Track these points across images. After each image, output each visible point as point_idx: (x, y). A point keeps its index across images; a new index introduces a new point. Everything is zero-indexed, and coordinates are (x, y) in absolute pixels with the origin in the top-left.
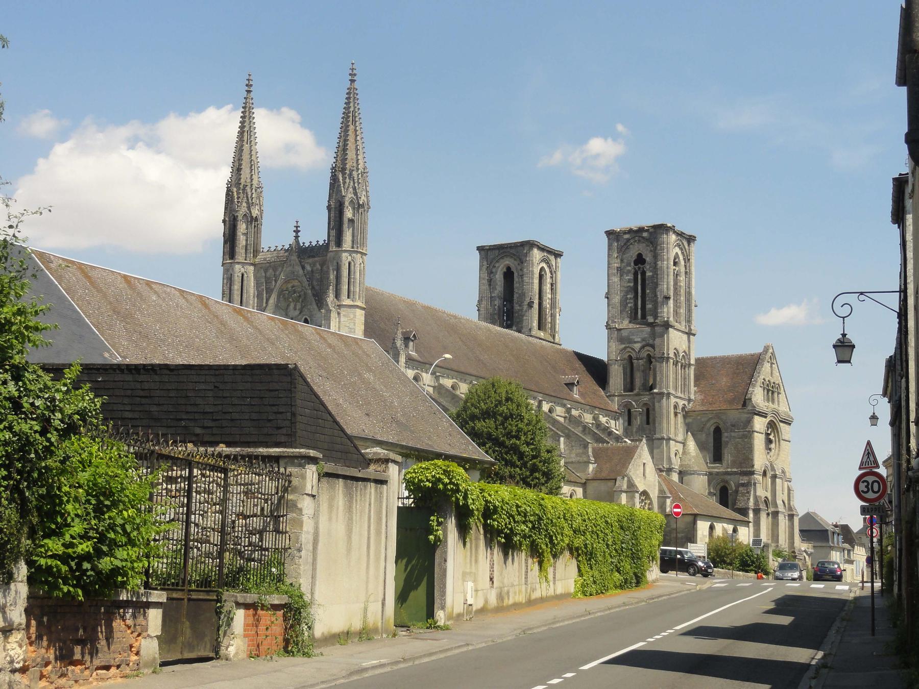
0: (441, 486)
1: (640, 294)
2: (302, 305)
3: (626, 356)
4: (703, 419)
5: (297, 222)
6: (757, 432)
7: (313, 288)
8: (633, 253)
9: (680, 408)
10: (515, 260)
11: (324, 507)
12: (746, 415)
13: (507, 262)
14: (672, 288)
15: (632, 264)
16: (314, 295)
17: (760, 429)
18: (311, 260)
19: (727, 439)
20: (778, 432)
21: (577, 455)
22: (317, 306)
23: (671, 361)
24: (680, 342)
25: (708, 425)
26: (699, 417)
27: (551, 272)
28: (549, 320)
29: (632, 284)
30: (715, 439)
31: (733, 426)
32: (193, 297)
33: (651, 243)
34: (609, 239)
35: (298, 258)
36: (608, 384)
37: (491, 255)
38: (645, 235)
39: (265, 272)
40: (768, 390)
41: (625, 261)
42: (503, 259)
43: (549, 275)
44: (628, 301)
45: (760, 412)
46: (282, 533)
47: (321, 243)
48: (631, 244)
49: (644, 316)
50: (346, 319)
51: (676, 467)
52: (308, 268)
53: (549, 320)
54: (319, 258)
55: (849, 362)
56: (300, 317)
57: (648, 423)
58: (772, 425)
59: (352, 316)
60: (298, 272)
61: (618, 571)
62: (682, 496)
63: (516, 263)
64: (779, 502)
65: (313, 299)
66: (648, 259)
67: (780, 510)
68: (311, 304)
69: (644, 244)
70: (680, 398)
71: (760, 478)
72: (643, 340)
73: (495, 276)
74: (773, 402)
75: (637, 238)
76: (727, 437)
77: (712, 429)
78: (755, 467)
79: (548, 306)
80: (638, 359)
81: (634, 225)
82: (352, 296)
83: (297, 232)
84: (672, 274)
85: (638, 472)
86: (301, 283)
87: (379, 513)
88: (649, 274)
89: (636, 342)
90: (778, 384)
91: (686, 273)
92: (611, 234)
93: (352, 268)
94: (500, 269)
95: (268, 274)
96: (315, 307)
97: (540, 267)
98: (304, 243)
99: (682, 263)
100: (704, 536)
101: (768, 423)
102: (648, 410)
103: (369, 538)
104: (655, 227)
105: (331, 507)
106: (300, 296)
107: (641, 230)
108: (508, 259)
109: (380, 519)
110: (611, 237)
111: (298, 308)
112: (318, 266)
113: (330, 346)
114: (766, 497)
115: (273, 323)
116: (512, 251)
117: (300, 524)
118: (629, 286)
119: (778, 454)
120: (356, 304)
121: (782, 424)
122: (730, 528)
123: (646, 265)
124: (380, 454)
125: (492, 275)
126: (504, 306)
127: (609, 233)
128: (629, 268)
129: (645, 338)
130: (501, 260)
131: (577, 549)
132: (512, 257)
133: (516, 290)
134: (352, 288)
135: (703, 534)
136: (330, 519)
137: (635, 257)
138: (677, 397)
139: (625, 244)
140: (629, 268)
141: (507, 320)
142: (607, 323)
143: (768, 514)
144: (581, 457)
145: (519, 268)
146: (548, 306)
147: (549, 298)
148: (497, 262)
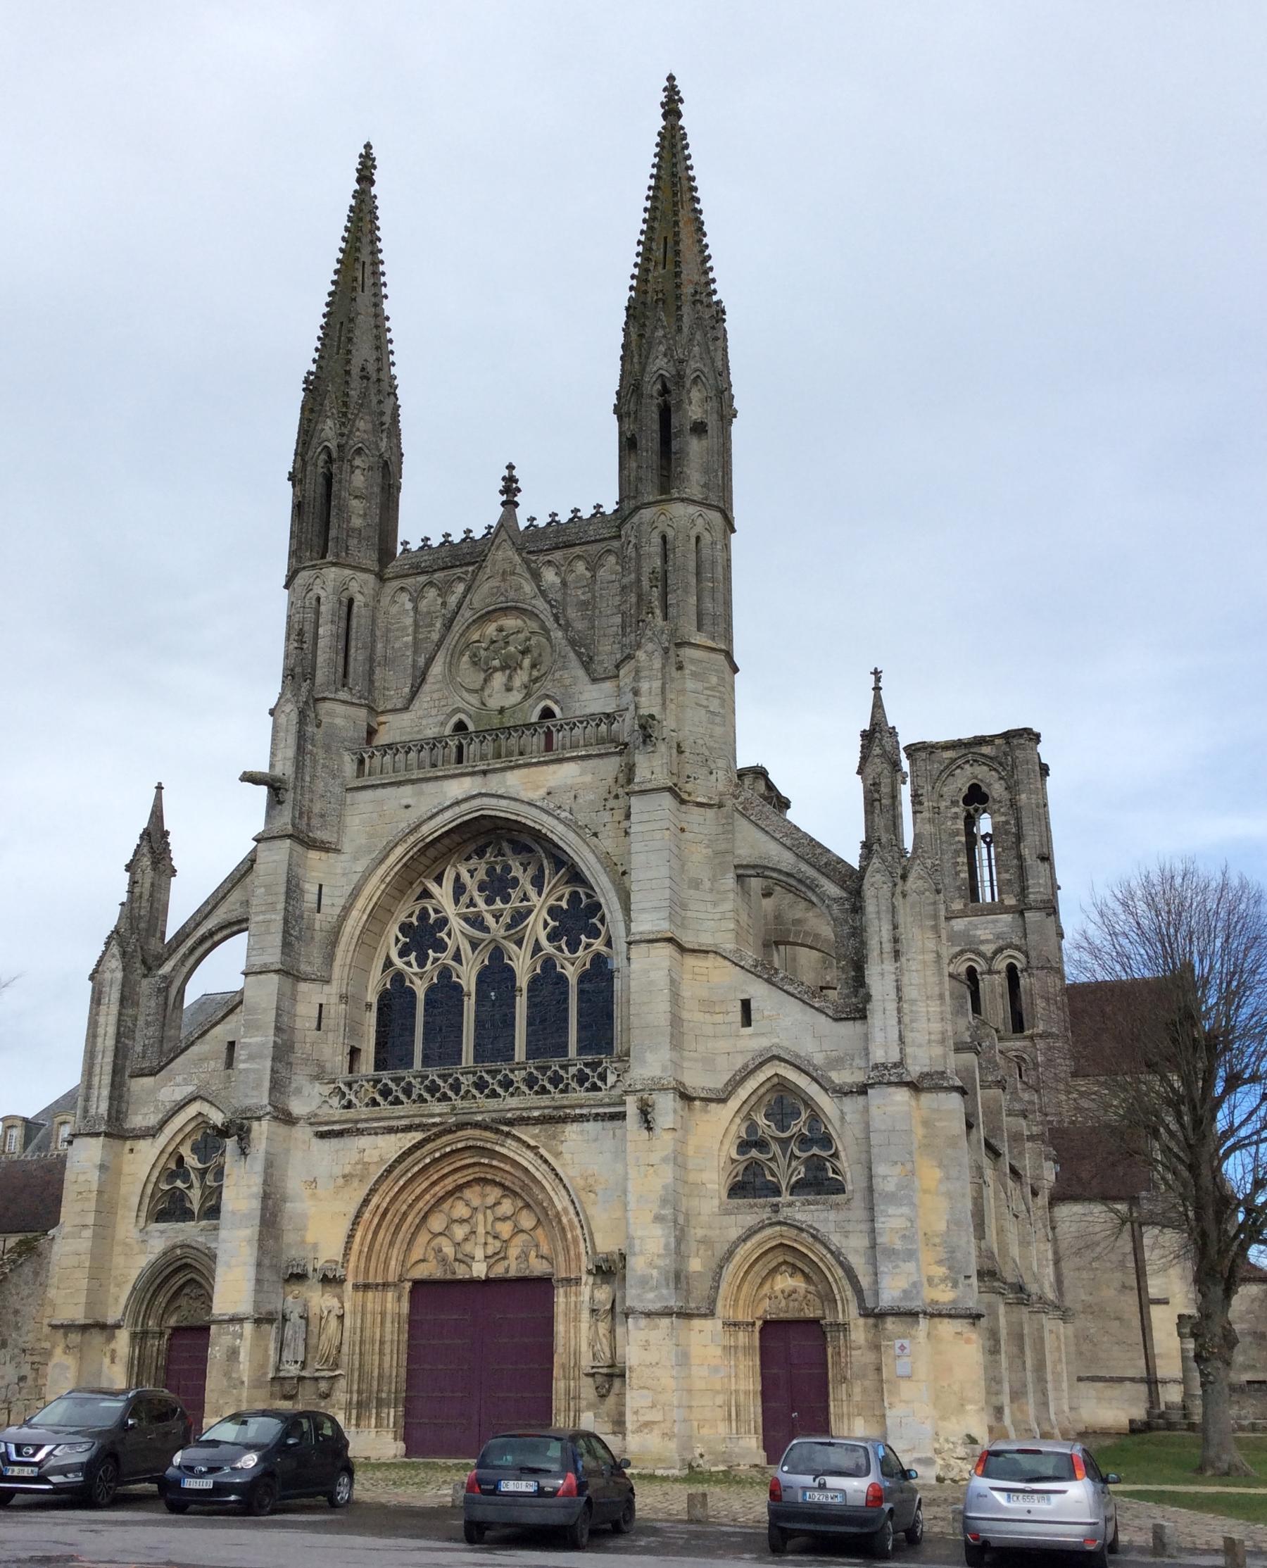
3: (963, 969)
8: (961, 782)
16: (572, 643)
18: (557, 556)
29: (963, 839)
33: (1001, 764)
38: (986, 750)
39: (414, 600)
48: (959, 767)
50: (699, 686)
52: (550, 576)
56: (527, 704)
59: (714, 680)
68: (564, 668)
72: (998, 937)
80: (990, 972)
81: (966, 733)
82: (708, 626)
89: (982, 942)
95: (423, 605)
96: (581, 673)
104: (1008, 736)
107: (980, 741)
123: (990, 803)
128: (955, 810)
137: (965, 790)
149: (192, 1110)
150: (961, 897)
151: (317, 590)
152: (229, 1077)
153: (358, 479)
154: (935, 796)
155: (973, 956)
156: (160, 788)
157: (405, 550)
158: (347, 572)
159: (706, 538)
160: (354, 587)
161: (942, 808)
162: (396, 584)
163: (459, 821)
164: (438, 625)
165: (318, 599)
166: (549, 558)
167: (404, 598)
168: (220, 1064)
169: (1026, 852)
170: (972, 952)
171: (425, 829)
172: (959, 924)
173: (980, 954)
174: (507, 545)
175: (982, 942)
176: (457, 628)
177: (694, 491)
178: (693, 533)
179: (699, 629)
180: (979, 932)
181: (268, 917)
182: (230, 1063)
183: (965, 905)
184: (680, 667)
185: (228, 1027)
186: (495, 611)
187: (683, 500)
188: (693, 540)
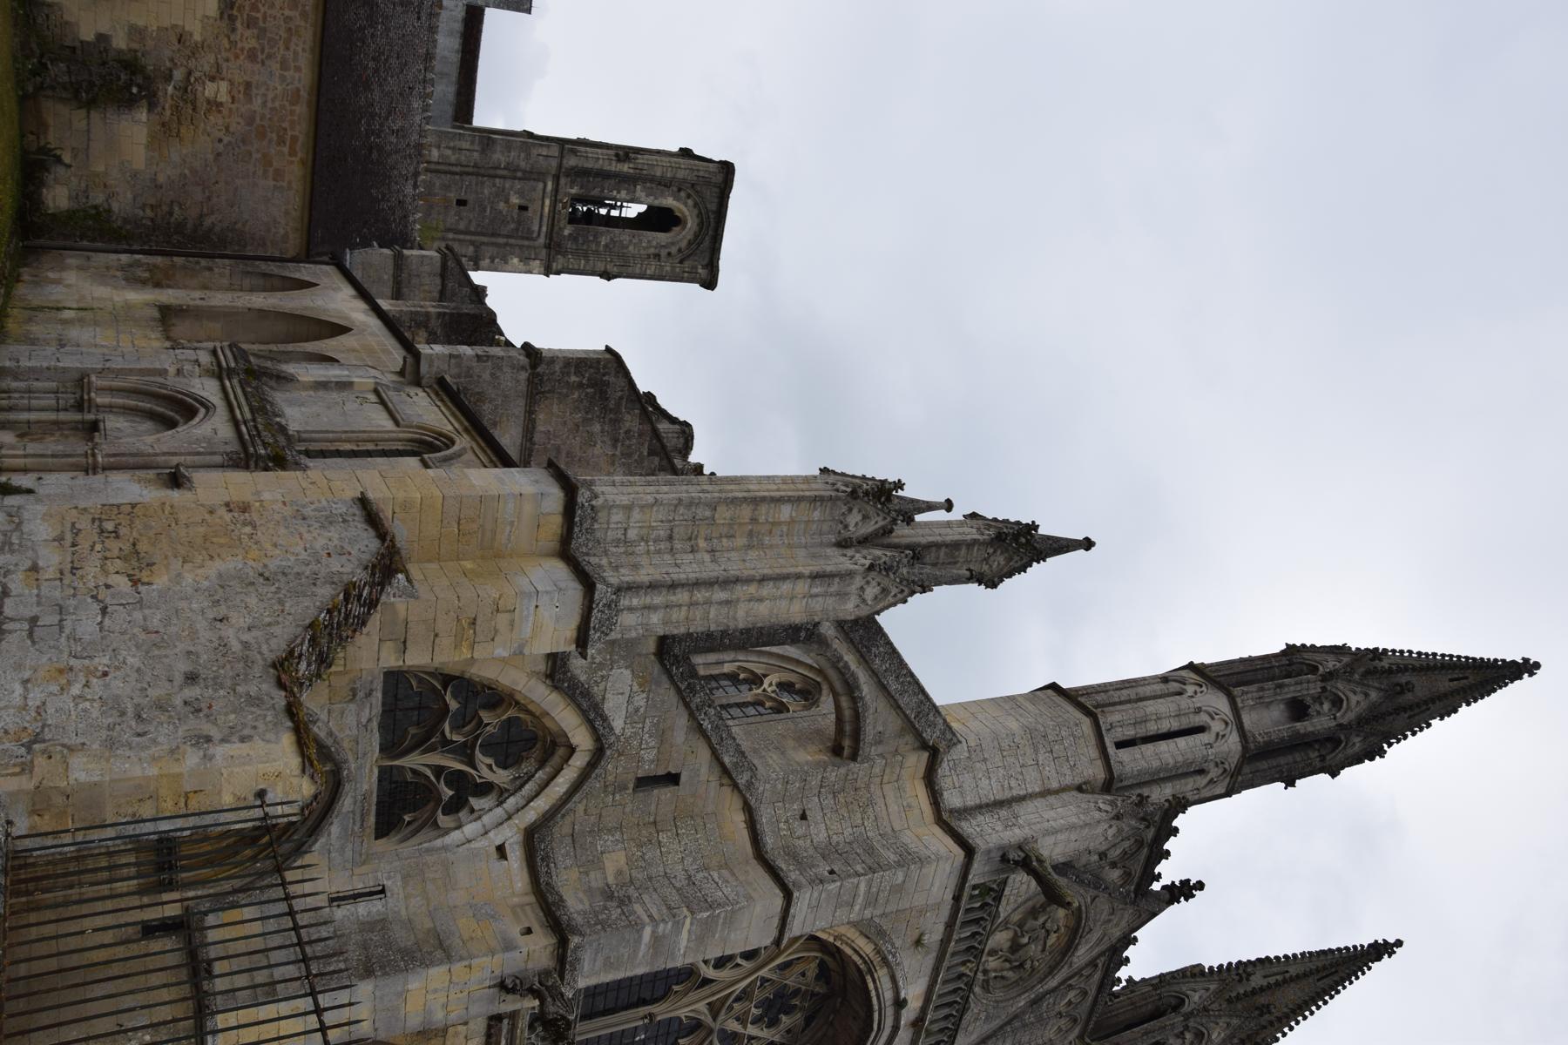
10: (690, 243)
13: (689, 225)
37: (710, 195)
42: (698, 216)
63: (684, 244)
108: (695, 228)
116: (707, 243)
130: (696, 212)
145: (674, 250)
148: (696, 205)
149: (581, 739)
152: (623, 788)
156: (1088, 544)
163: (876, 1007)
168: (647, 769)
171: (882, 974)
181: (860, 900)
182: (646, 782)
185: (704, 770)
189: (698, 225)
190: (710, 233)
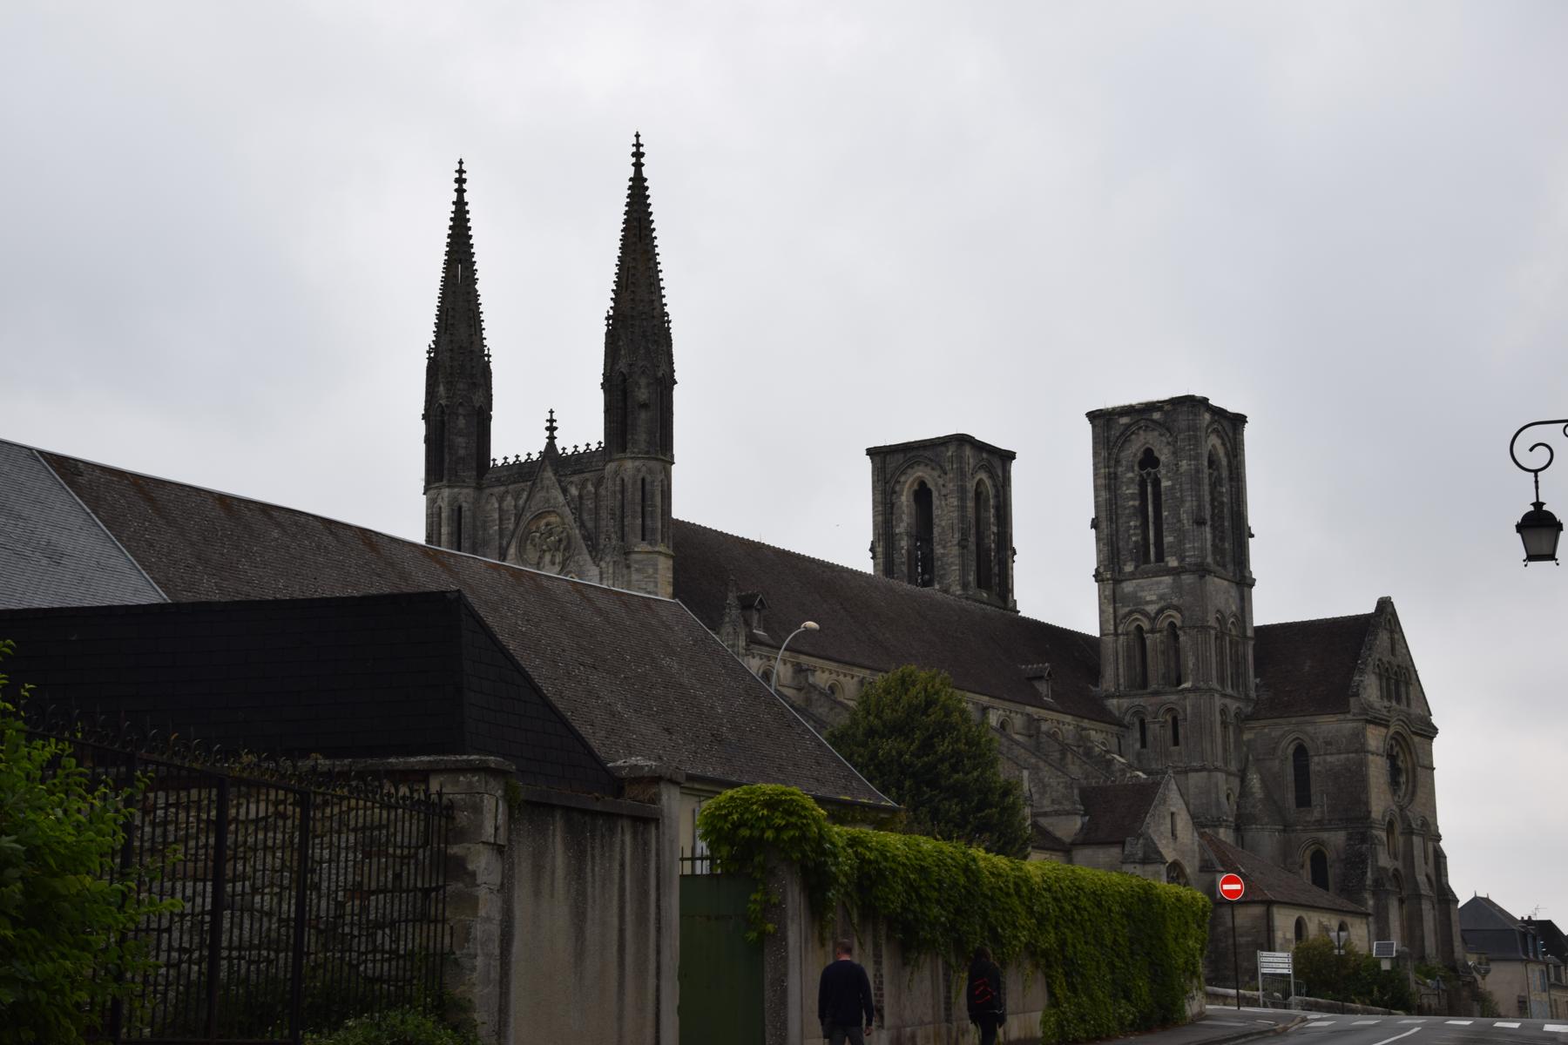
0: (769, 834)
1: (1151, 519)
2: (564, 555)
4: (1273, 734)
5: (551, 412)
6: (1373, 754)
7: (582, 525)
8: (1134, 449)
9: (1233, 714)
10: (933, 469)
11: (524, 869)
12: (1350, 725)
13: (920, 474)
14: (1208, 506)
15: (1136, 468)
17: (1378, 748)
18: (575, 478)
19: (1318, 768)
20: (1411, 753)
21: (1053, 802)
22: (591, 556)
23: (1213, 632)
24: (1227, 600)
25: (1284, 743)
26: (1266, 730)
27: (995, 486)
28: (996, 569)
29: (1137, 503)
30: (1296, 768)
31: (1328, 743)
32: (348, 533)
33: (1168, 429)
34: (1094, 427)
35: (555, 474)
36: (1103, 676)
38: (1156, 416)
40: (1388, 679)
41: (1124, 463)
42: (912, 468)
43: (991, 492)
44: (1132, 532)
45: (1376, 718)
46: (436, 921)
47: (594, 447)
48: (1133, 433)
49: (1160, 557)
51: (1231, 819)
52: (574, 491)
53: (996, 569)
54: (592, 474)
55: (1551, 557)
57: (1176, 743)
58: (1399, 738)
59: (651, 571)
60: (556, 498)
61: (1127, 997)
62: (1243, 870)
63: (936, 474)
64: (1421, 878)
65: (584, 546)
66: (1163, 458)
67: (1423, 892)
68: (580, 554)
69: (1156, 433)
70: (1231, 697)
71: (1383, 835)
72: (1161, 597)
73: (899, 497)
74: (1398, 701)
75: (1142, 423)
76: (1318, 764)
77: (1291, 751)
78: (1373, 815)
79: (993, 546)
80: (1152, 631)
83: (551, 429)
84: (1206, 481)
85: (1162, 828)
86: (562, 518)
87: (642, 882)
88: (1165, 483)
89: (1148, 603)
90: (1407, 668)
91: (1231, 479)
92: (1099, 419)
93: (648, 487)
94: (907, 485)
95: (505, 505)
97: (978, 478)
98: (564, 449)
99: (1224, 462)
100: (1287, 941)
101: (1392, 738)
102: (1175, 720)
103: (622, 931)
105: (538, 869)
106: (560, 541)
108: (922, 467)
109: (643, 894)
110: (1097, 422)
111: (557, 561)
112: (590, 488)
113: (599, 611)
114: (1396, 870)
115: (495, 575)
116: (928, 454)
117: (473, 902)
118: (1133, 506)
119: (1414, 793)
120: (657, 549)
121: (1417, 739)
122: (1333, 922)
124: (642, 767)
125: (894, 496)
126: (919, 548)
127: (1093, 416)
128: (1130, 475)
129: (1164, 594)
130: (909, 471)
131: (1045, 954)
132: (927, 465)
133: (936, 521)
134: (649, 522)
135: (1285, 938)
136: (537, 893)
137: (1140, 455)
138: (1224, 696)
139: (1122, 434)
140: (1130, 475)
141: (923, 573)
142: (1096, 570)
143: (1401, 901)
144: (1060, 803)
145: (941, 482)
146: (993, 546)
147: (993, 533)
148: (903, 473)
150: (1132, 560)
151: (439, 502)
153: (462, 422)
154: (1112, 463)
155: (1140, 617)
157: (494, 465)
158: (456, 490)
159: (648, 479)
160: (462, 498)
161: (1119, 473)
162: (488, 491)
164: (513, 519)
165: (440, 508)
166: (572, 479)
167: (494, 500)
169: (1184, 516)
170: (1139, 612)
172: (1128, 587)
173: (1146, 614)
174: (549, 469)
175: (1148, 603)
176: (522, 524)
177: (643, 446)
178: (640, 477)
179: (643, 539)
180: (1143, 594)
183: (1136, 567)
184: (628, 567)
186: (542, 513)
187: (632, 458)
188: (639, 483)
189: (919, 465)
190: (921, 453)
